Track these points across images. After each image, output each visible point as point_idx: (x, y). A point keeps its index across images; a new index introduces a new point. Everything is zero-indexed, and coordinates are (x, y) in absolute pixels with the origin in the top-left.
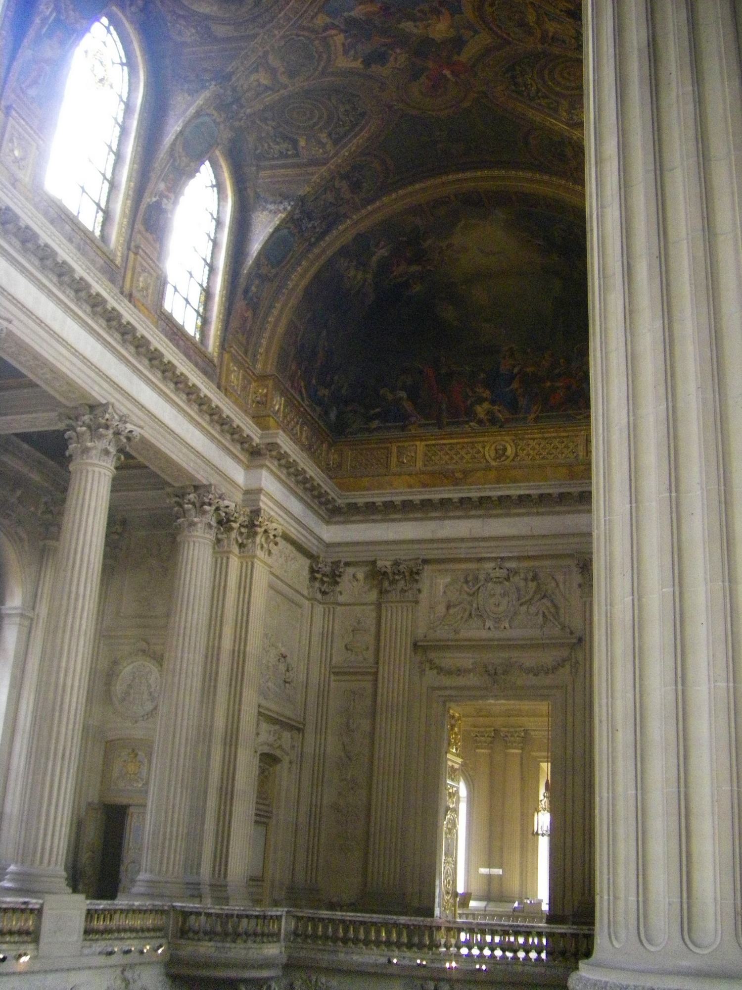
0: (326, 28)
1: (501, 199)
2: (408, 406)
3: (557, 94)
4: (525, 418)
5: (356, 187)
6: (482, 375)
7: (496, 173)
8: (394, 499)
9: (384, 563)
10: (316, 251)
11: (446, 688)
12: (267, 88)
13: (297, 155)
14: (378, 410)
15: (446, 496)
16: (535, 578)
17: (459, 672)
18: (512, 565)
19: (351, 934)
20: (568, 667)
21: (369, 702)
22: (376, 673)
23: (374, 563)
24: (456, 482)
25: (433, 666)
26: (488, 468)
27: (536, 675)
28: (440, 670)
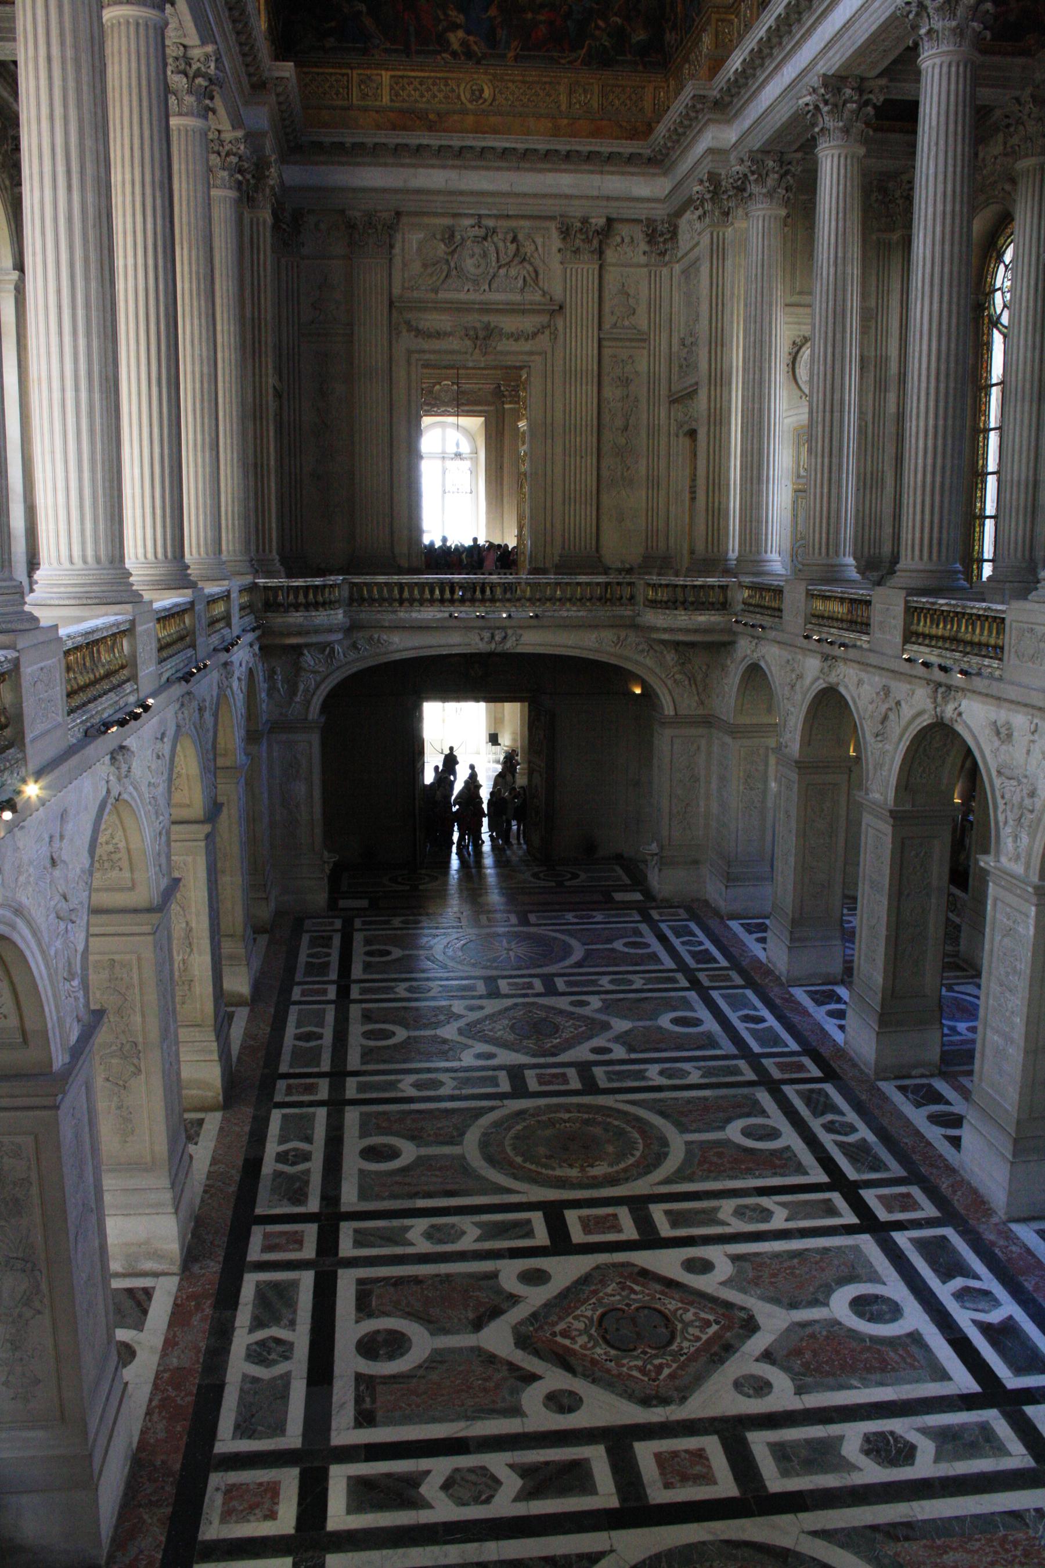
2: (368, 22)
4: (504, 56)
8: (365, 140)
11: (424, 352)
14: (333, 24)
15: (425, 142)
16: (514, 239)
17: (438, 335)
18: (490, 223)
19: (406, 594)
20: (547, 332)
23: (343, 212)
25: (410, 328)
26: (464, 112)
27: (516, 340)
28: (419, 332)
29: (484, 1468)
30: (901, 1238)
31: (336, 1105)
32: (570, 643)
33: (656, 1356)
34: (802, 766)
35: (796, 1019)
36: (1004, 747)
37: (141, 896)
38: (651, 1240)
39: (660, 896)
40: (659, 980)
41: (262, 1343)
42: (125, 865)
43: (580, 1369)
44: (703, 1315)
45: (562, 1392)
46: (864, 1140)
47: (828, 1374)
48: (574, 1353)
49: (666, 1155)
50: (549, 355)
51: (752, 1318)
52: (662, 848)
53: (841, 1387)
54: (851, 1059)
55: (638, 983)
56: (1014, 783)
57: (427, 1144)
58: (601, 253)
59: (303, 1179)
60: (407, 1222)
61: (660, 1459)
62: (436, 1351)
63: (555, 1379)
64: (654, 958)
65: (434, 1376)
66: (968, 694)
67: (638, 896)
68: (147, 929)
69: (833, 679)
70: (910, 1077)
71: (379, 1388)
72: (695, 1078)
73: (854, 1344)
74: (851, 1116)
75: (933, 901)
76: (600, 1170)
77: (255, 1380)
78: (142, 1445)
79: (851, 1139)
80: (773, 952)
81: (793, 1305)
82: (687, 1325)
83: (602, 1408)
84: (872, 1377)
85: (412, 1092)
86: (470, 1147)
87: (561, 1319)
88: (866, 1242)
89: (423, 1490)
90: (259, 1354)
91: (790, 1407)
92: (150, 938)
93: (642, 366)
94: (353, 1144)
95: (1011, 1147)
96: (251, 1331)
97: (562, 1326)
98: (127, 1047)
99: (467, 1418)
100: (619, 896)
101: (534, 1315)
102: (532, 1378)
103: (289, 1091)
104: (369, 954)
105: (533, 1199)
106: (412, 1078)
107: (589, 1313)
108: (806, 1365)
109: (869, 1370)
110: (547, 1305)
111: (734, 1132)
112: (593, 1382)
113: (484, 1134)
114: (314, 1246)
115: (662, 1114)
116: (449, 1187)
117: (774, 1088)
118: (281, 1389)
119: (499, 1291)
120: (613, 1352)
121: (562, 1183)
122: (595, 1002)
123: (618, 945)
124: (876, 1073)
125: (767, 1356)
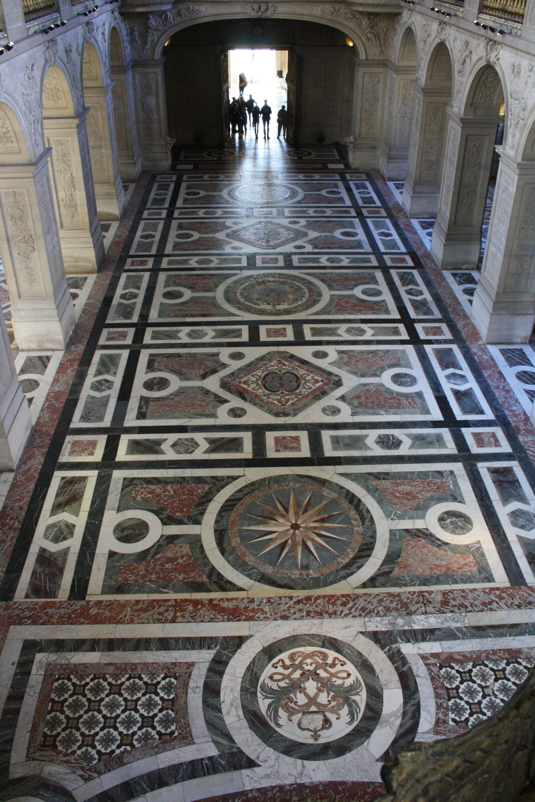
29: (193, 439)
30: (428, 348)
31: (155, 271)
33: (288, 395)
34: (426, 92)
35: (408, 235)
36: (515, 80)
37: (24, 158)
38: (300, 341)
39: (353, 166)
40: (340, 212)
41: (99, 382)
42: (14, 139)
43: (249, 399)
44: (316, 377)
45: (237, 408)
46: (425, 299)
47: (370, 407)
48: (247, 391)
49: (319, 301)
51: (340, 380)
52: (355, 140)
53: (375, 414)
54: (432, 258)
55: (329, 212)
56: (517, 102)
57: (197, 291)
59: (132, 307)
60: (180, 328)
61: (277, 440)
62: (181, 388)
63: (236, 402)
64: (341, 200)
65: (178, 399)
66: (504, 47)
67: (342, 166)
68: (29, 175)
69: (443, 37)
70: (461, 269)
71: (151, 403)
72: (345, 263)
73: (387, 395)
74: (422, 287)
75: (482, 172)
76: (281, 307)
77: (93, 398)
78: (37, 423)
79: (419, 298)
80: (402, 198)
81: (363, 376)
82: (306, 381)
83: (255, 416)
84: (392, 411)
85: (195, 265)
86: (219, 294)
87: (245, 376)
88: (410, 350)
89: (163, 447)
90: (97, 386)
91: (346, 421)
92: (32, 180)
94: (160, 289)
95: (492, 306)
96: (95, 376)
97: (245, 379)
98: (27, 237)
99: (190, 418)
100: (331, 166)
101: (233, 374)
102: (224, 401)
103: (133, 264)
104: (188, 194)
105: (245, 319)
106: (197, 258)
107: (259, 374)
108: (360, 404)
109: (391, 407)
110: (240, 369)
111: (358, 292)
112: (254, 404)
113: (228, 287)
114: (132, 338)
115: (323, 280)
116: (204, 312)
117: (385, 270)
118: (104, 402)
119: (218, 362)
120: (267, 392)
121: (262, 312)
122: (303, 222)
123: (324, 192)
124: (442, 266)
125: (343, 398)
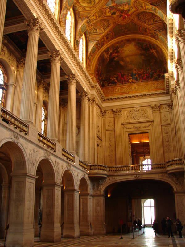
0: (106, 8)
1: (134, 40)
2: (116, 81)
3: (146, 19)
5: (107, 38)
6: (130, 74)
7: (133, 35)
9: (114, 110)
10: (100, 51)
12: (95, 19)
13: (97, 32)
14: (110, 82)
17: (130, 128)
21: (114, 136)
22: (115, 130)
24: (127, 94)
25: (126, 128)
27: (145, 128)
28: (127, 128)
32: (153, 177)
50: (152, 130)
58: (160, 110)
93: (170, 129)
